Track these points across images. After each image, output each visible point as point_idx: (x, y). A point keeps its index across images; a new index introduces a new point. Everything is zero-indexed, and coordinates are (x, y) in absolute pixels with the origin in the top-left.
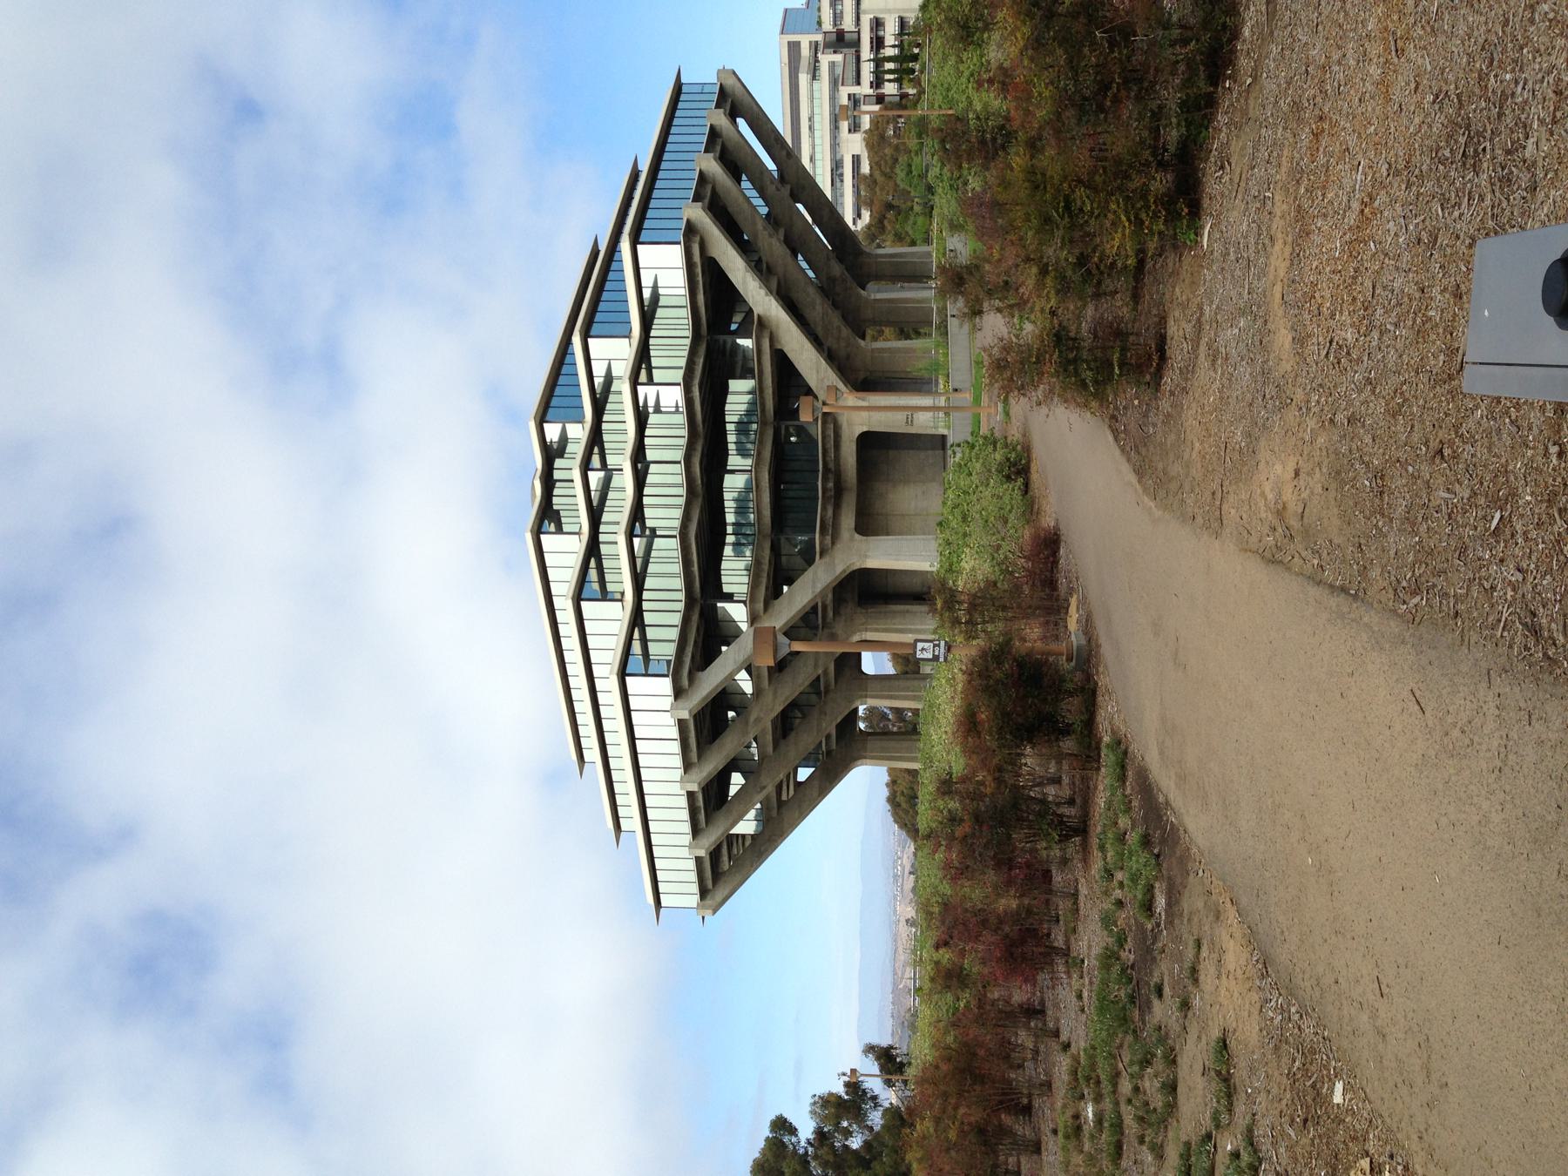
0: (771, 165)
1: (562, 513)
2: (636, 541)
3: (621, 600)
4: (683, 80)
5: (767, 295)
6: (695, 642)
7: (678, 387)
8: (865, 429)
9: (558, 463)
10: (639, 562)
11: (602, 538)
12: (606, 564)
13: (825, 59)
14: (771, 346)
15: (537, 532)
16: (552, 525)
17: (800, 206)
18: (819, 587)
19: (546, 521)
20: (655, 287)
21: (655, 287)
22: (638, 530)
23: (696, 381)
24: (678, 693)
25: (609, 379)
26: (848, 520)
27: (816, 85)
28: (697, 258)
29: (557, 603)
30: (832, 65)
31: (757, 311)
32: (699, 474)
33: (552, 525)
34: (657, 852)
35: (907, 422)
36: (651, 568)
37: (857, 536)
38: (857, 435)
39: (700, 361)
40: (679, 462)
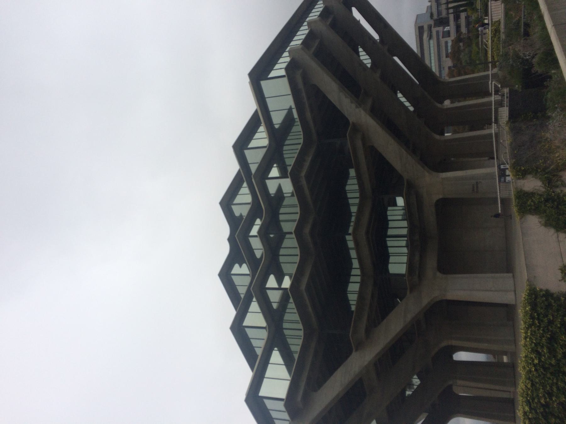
0: (376, 36)
5: (357, 107)
8: (441, 197)
13: (434, 30)
14: (364, 144)
17: (396, 58)
18: (409, 317)
23: (303, 174)
26: (431, 262)
27: (431, 42)
28: (301, 85)
30: (438, 32)
31: (352, 119)
35: (473, 190)
37: (439, 274)
38: (434, 202)
39: (309, 159)
40: (291, 233)
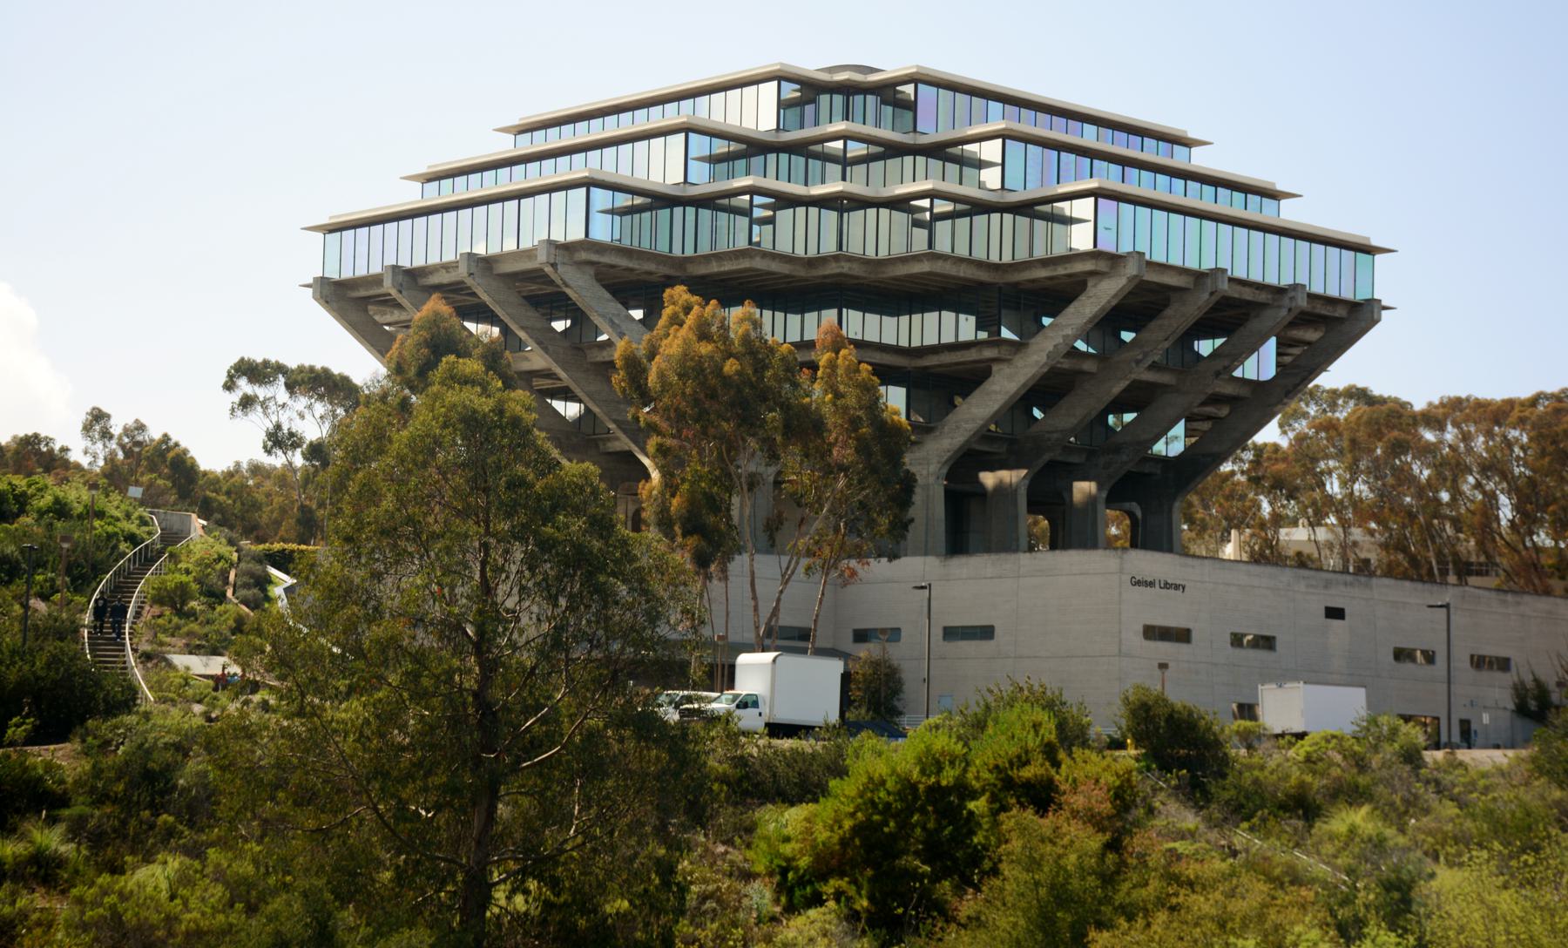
1: (809, 109)
2: (747, 197)
3: (686, 181)
4: (1378, 257)
6: (631, 270)
7: (926, 247)
9: (871, 100)
10: (726, 201)
11: (772, 157)
12: (740, 164)
15: (780, 77)
16: (799, 94)
19: (798, 87)
20: (1069, 221)
21: (1069, 221)
22: (758, 200)
24: (568, 248)
25: (963, 161)
28: (1079, 267)
29: (687, 105)
32: (827, 272)
33: (799, 94)
34: (391, 227)
36: (723, 216)
